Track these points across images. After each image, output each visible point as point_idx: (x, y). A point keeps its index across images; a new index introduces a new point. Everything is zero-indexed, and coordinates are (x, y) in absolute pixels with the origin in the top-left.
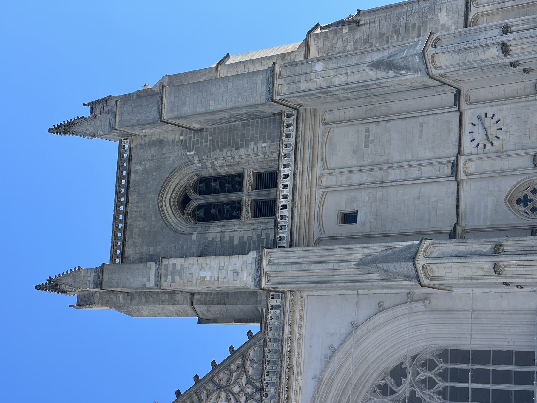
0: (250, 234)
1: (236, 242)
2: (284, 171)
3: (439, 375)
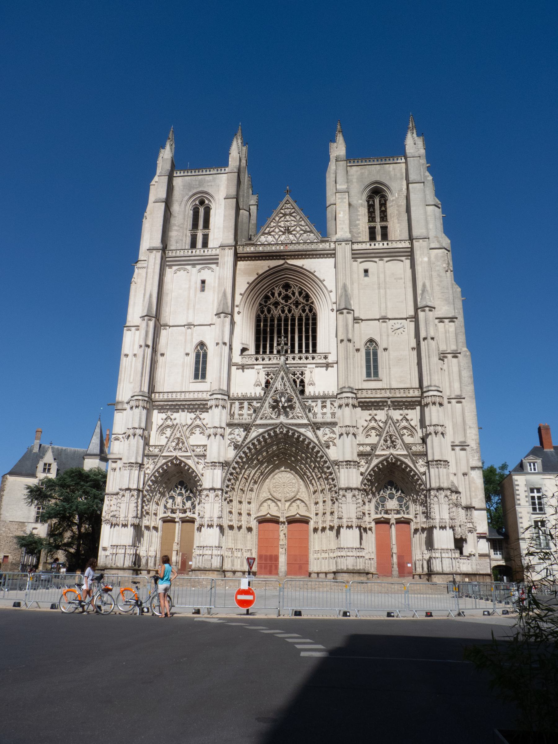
0: (361, 229)
1: (357, 222)
2: (385, 243)
3: (307, 314)
